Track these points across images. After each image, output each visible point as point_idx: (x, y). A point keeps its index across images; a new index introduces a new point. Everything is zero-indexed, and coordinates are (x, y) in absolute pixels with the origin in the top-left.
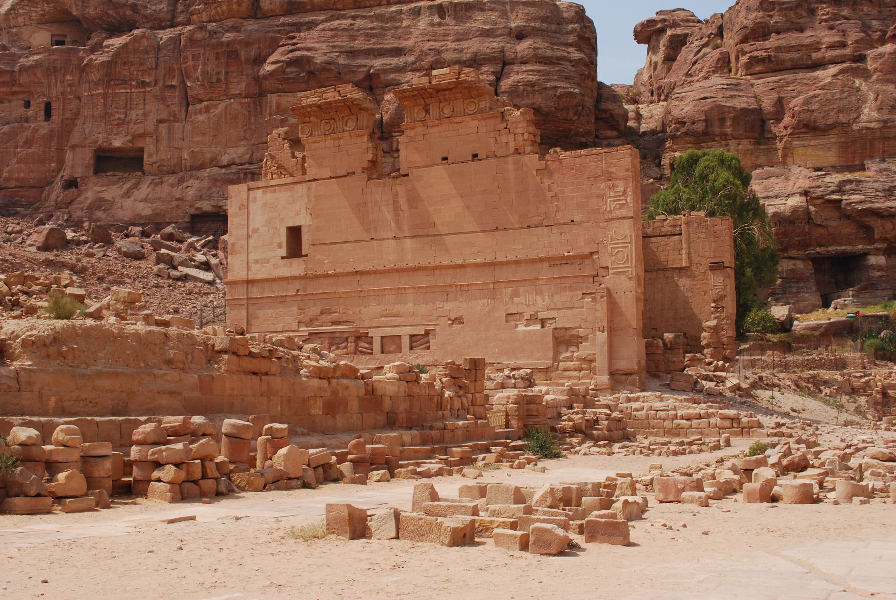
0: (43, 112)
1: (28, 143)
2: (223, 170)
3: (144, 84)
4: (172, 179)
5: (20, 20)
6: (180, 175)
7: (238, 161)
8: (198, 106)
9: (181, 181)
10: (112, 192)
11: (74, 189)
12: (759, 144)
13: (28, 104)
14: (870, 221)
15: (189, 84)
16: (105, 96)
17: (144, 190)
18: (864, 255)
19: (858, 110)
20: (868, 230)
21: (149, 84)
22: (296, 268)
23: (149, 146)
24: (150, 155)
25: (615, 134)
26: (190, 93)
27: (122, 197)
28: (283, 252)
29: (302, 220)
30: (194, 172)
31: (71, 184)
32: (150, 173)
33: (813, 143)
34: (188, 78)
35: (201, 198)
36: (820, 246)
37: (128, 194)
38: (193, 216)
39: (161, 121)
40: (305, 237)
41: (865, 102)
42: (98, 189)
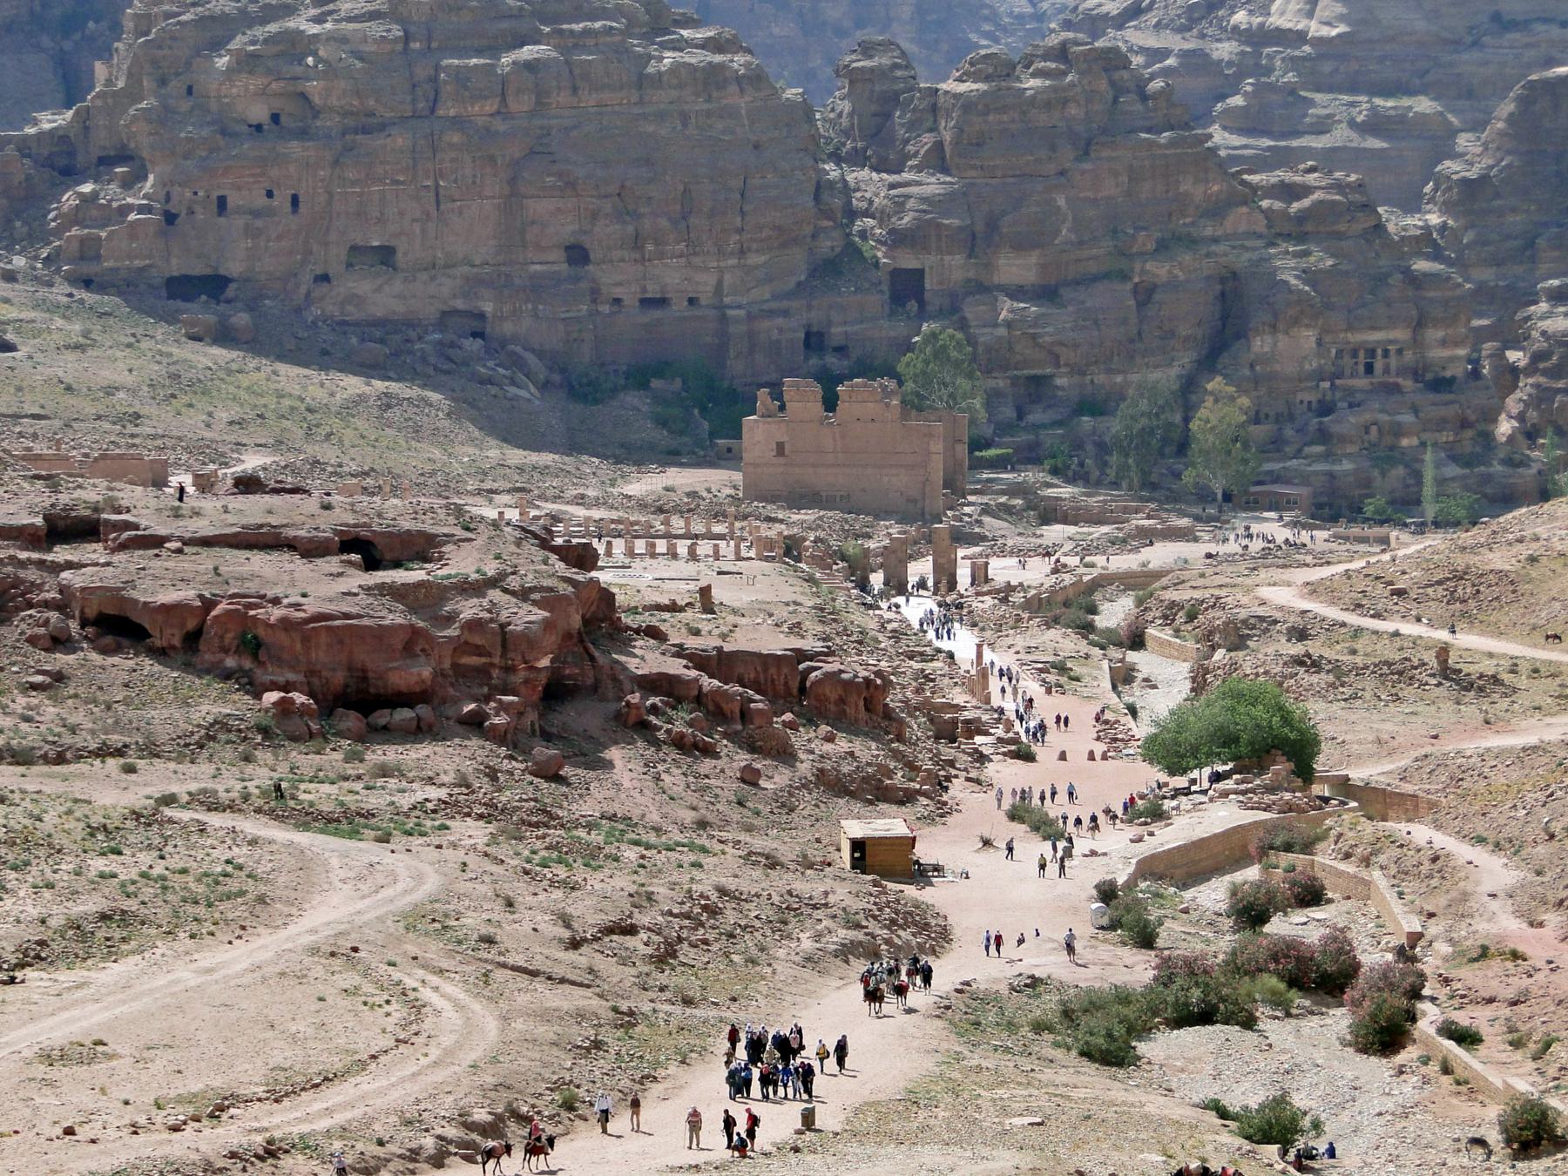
0: (289, 205)
1: (279, 238)
2: (476, 270)
3: (397, 182)
4: (424, 276)
5: (234, 90)
6: (433, 272)
7: (491, 262)
8: (450, 205)
9: (433, 279)
10: (364, 287)
11: (325, 284)
12: (970, 257)
13: (270, 194)
14: (1058, 349)
15: (442, 183)
16: (361, 194)
17: (398, 286)
18: (1051, 377)
19: (1057, 232)
20: (1057, 357)
21: (402, 183)
22: (782, 460)
23: (401, 246)
24: (405, 254)
25: (831, 223)
26: (442, 192)
27: (374, 291)
28: (774, 453)
29: (785, 439)
30: (447, 271)
31: (324, 278)
32: (402, 270)
33: (1018, 262)
34: (442, 177)
35: (455, 296)
36: (1016, 369)
37: (379, 289)
38: (444, 313)
39: (414, 220)
40: (787, 447)
41: (1064, 222)
42: (351, 285)
